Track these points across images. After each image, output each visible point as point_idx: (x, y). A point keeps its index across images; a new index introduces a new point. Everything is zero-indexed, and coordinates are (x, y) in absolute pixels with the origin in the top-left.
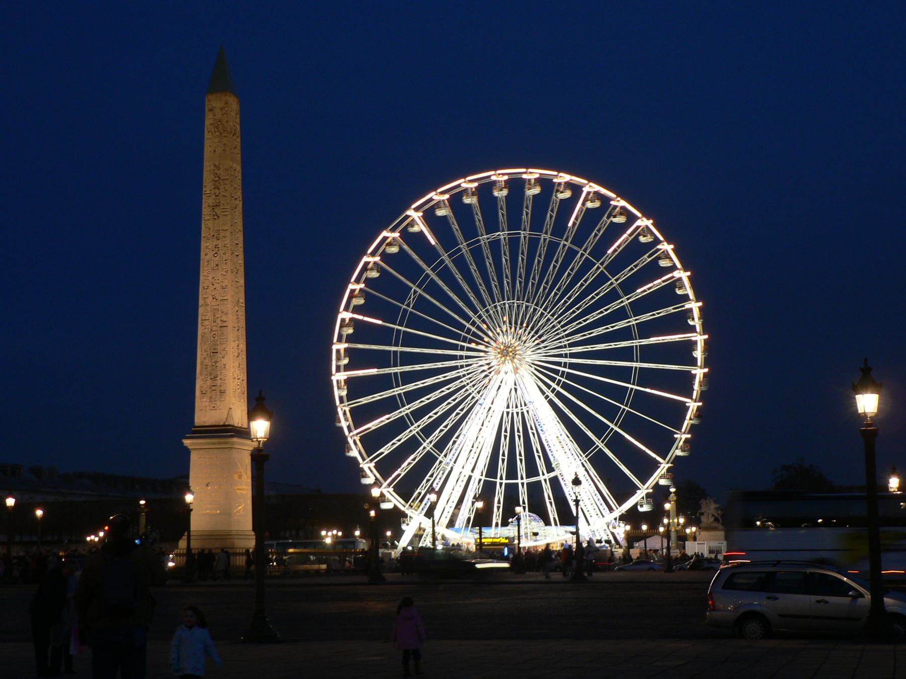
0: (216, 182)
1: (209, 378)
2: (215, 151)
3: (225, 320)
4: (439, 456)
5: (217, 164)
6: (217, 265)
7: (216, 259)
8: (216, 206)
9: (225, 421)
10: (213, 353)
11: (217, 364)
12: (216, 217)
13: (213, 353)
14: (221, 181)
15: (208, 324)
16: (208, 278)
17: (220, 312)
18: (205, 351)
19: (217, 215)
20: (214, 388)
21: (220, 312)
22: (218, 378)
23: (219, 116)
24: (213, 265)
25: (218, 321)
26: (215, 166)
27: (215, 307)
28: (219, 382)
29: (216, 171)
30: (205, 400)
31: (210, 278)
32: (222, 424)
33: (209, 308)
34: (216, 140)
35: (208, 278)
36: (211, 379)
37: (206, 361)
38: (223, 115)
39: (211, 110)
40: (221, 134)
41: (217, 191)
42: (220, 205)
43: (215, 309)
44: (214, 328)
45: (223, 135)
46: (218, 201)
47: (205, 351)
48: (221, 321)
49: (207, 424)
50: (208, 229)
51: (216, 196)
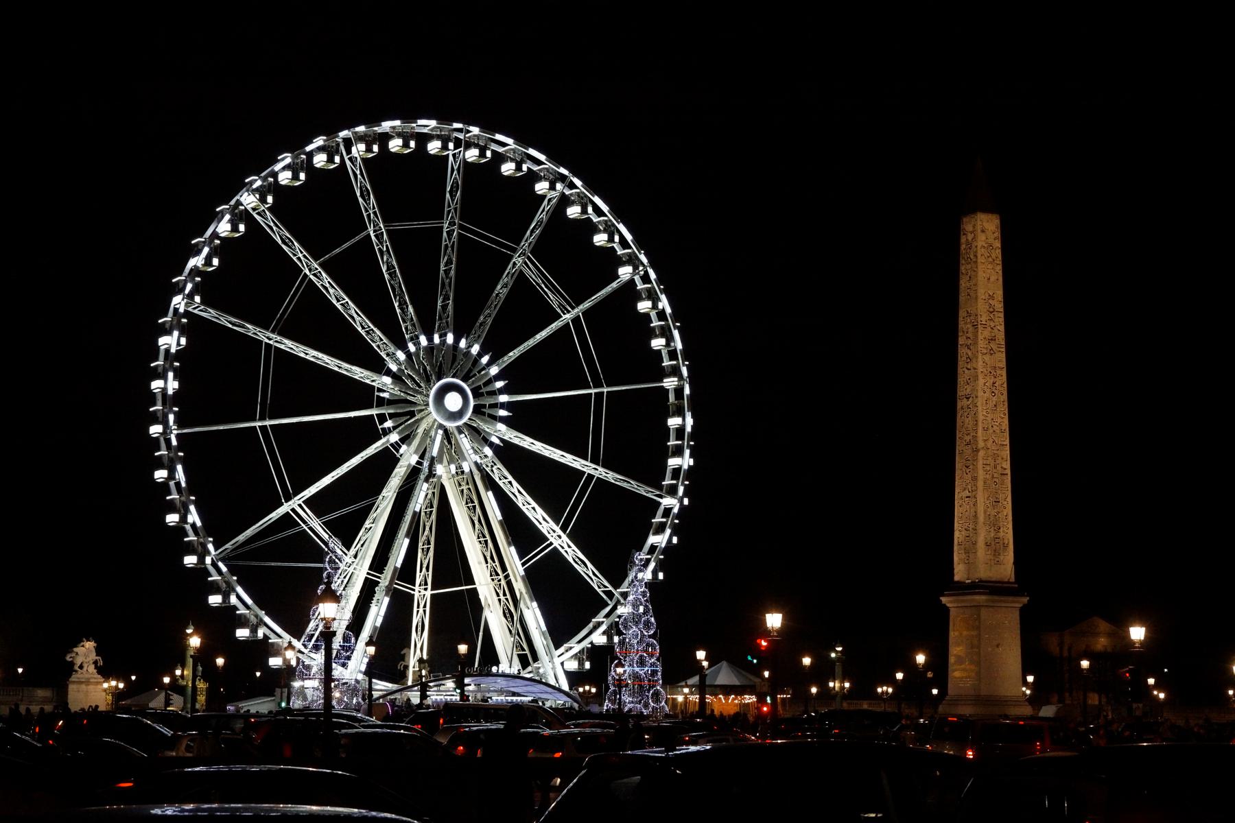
0: (991, 312)
1: (993, 531)
2: (989, 279)
3: (1005, 467)
4: (414, 590)
5: (991, 294)
6: (995, 406)
7: (994, 399)
8: (992, 340)
9: (1008, 578)
10: (995, 502)
11: (1000, 514)
12: (992, 351)
13: (995, 502)
14: (995, 313)
15: (988, 469)
16: (987, 418)
17: (1000, 458)
18: (988, 499)
19: (992, 349)
20: (997, 540)
21: (1000, 458)
22: (1001, 530)
23: (991, 240)
24: (991, 404)
25: (999, 467)
26: (990, 295)
27: (995, 452)
28: (1001, 534)
29: (991, 301)
30: (989, 552)
31: (989, 419)
32: (1006, 580)
33: (990, 452)
34: (990, 266)
35: (987, 418)
36: (995, 530)
37: (989, 510)
38: (995, 239)
39: (983, 231)
40: (994, 260)
41: (992, 324)
42: (995, 340)
43: (995, 454)
44: (995, 475)
45: (995, 262)
46: (993, 335)
47: (988, 499)
48: (1002, 467)
49: (993, 580)
50: (985, 364)
51: (992, 328)
